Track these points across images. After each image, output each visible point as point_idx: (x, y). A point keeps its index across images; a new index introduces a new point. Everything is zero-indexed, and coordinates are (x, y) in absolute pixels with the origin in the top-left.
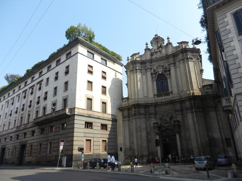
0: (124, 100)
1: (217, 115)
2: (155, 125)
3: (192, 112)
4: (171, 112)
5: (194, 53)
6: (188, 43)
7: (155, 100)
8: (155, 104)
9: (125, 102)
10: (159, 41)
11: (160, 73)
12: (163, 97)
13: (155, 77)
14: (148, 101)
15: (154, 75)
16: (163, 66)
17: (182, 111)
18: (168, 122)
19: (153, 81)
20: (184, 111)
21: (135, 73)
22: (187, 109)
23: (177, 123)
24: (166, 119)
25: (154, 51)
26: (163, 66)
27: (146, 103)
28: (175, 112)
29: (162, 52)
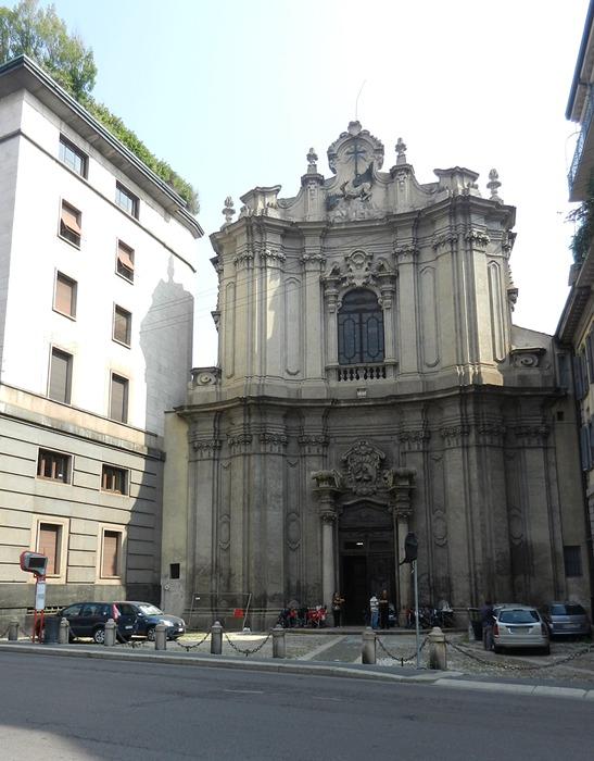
0: (202, 378)
1: (547, 463)
2: (323, 485)
3: (466, 447)
4: (385, 441)
5: (497, 220)
6: (474, 176)
7: (329, 390)
8: (327, 404)
9: (205, 384)
10: (364, 152)
11: (359, 283)
12: (361, 379)
13: (336, 296)
14: (299, 391)
15: (331, 290)
16: (371, 257)
17: (427, 439)
18: (371, 477)
19: (325, 311)
20: (435, 442)
21: (257, 271)
22: (448, 435)
23: (407, 483)
24: (368, 466)
25: (341, 193)
26: (371, 257)
27: (293, 396)
28: (402, 441)
29: (372, 200)
